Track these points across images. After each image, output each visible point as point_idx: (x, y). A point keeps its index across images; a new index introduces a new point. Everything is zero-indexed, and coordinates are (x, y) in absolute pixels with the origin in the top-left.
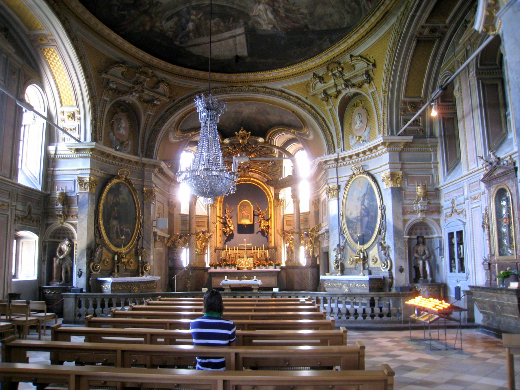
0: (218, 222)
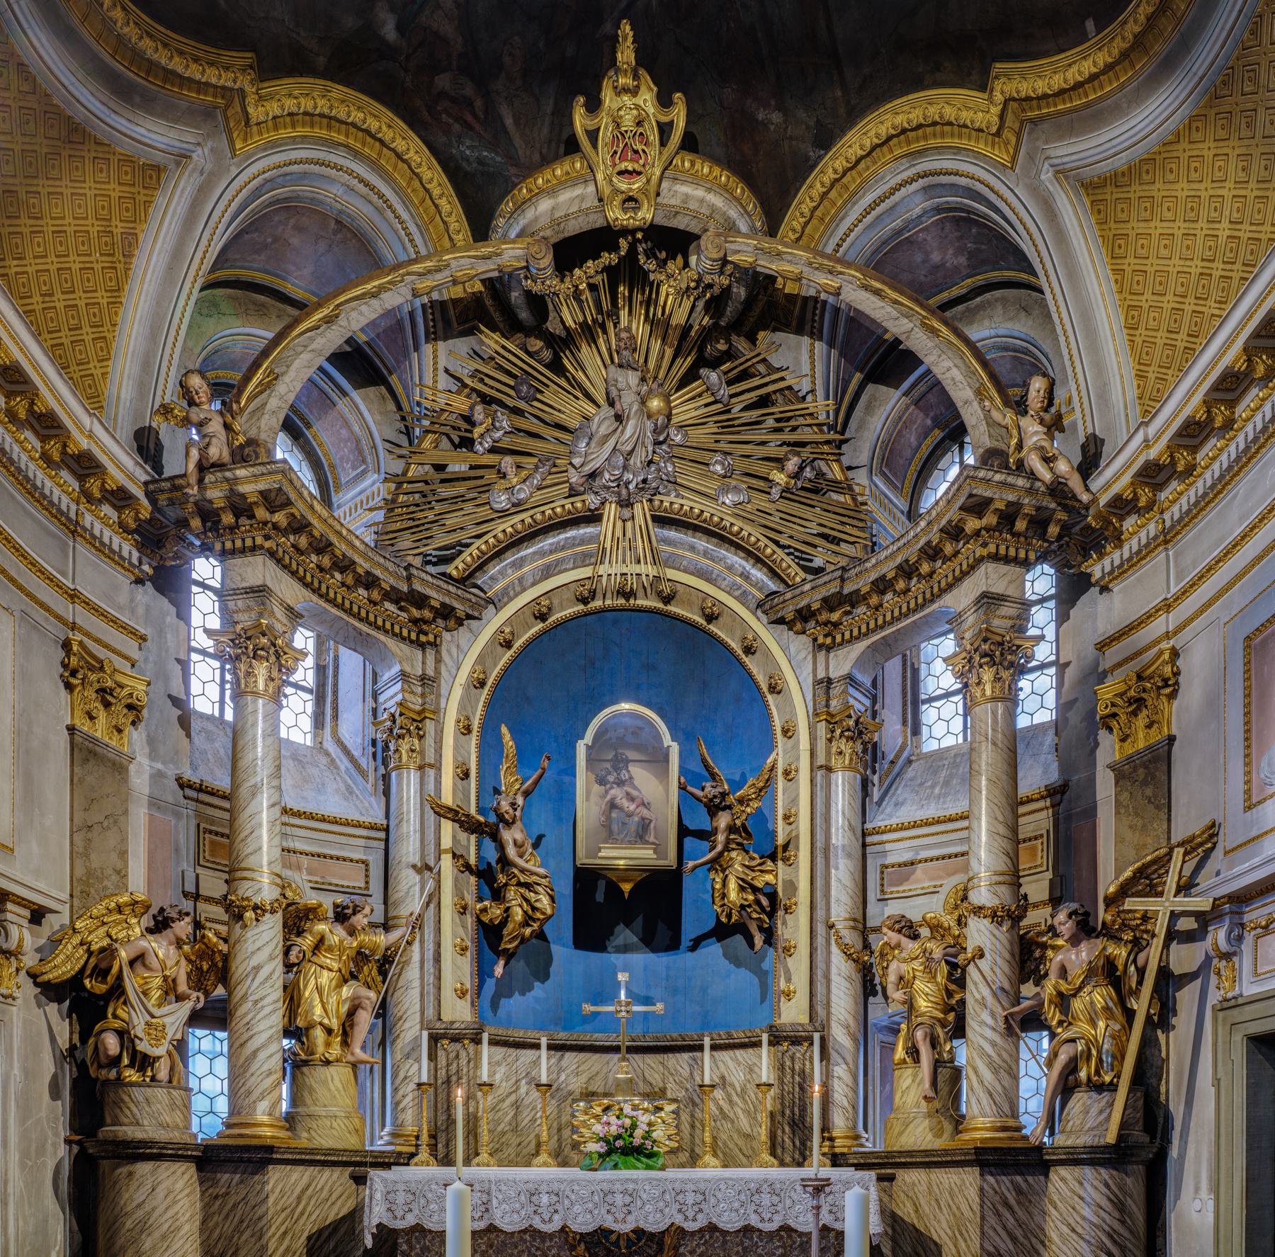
0: (447, 861)
